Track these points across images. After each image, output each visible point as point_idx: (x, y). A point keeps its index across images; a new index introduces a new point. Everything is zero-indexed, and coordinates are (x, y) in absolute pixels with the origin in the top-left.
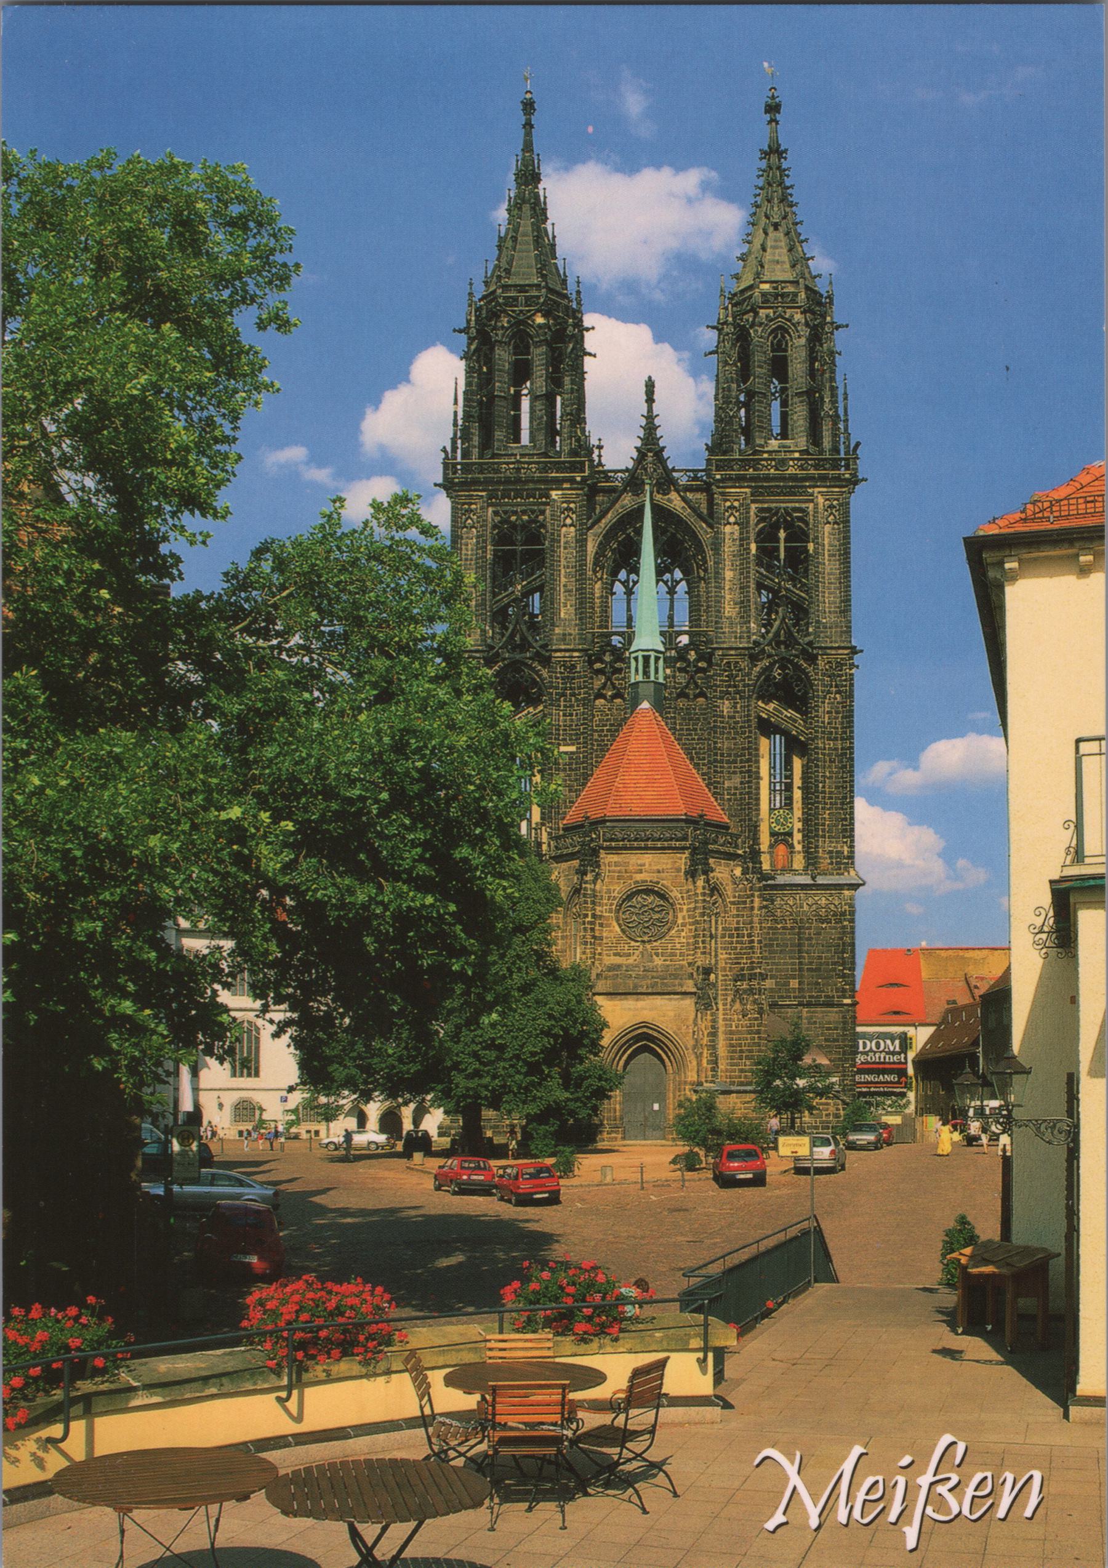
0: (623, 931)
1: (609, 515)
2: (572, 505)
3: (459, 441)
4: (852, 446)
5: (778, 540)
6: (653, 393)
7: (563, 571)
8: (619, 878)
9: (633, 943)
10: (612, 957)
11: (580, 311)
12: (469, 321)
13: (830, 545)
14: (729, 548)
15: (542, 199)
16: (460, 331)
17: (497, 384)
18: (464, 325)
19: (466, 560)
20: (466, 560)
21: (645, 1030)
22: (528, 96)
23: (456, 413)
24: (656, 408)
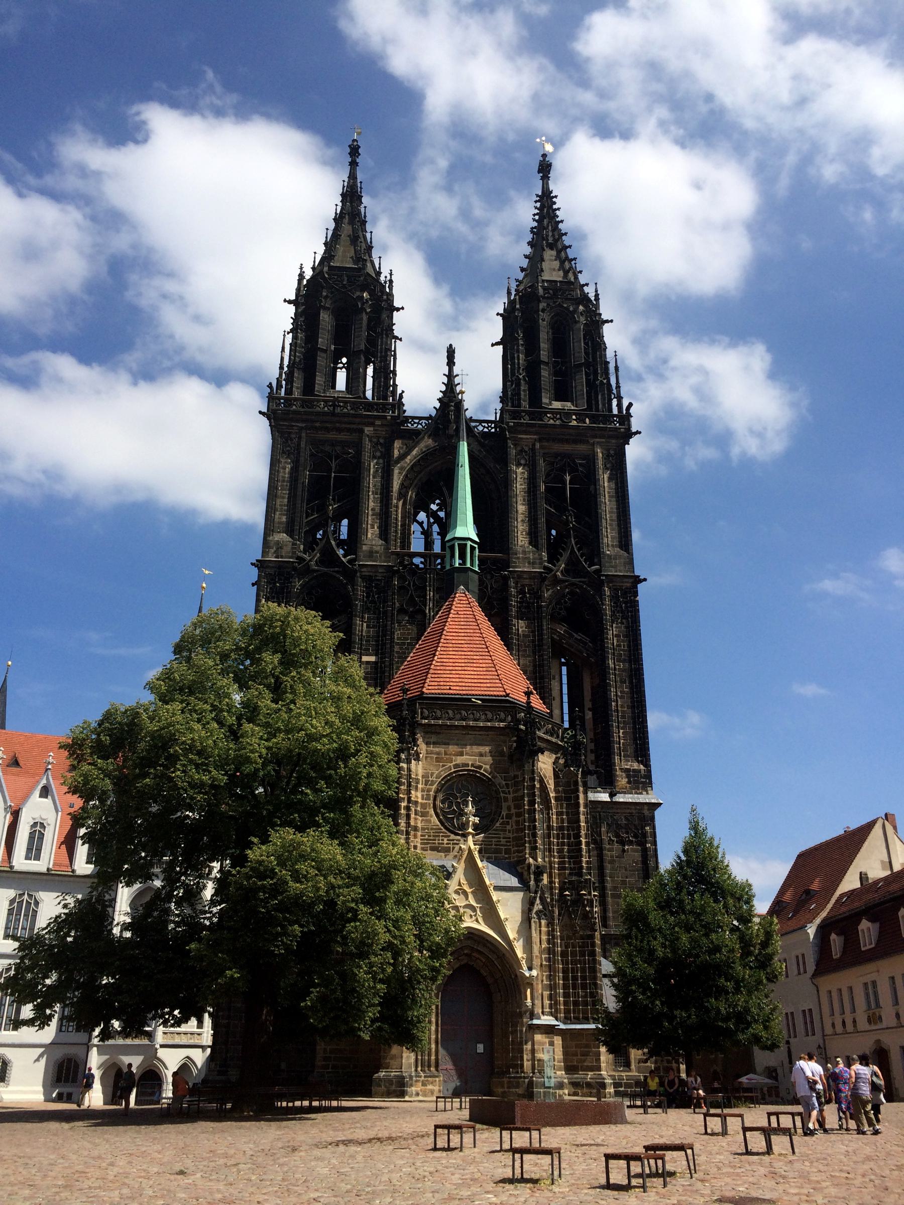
0: (440, 821)
1: (414, 452)
2: (382, 441)
3: (284, 383)
4: (624, 408)
5: (564, 482)
6: (454, 357)
7: (371, 497)
8: (438, 760)
9: (452, 836)
10: (429, 852)
11: (391, 295)
12: (297, 295)
13: (609, 488)
14: (519, 486)
15: (363, 214)
16: (290, 302)
17: (320, 340)
18: (293, 297)
19: (283, 481)
20: (283, 481)
21: (469, 943)
22: (355, 143)
23: (282, 359)
24: (456, 370)
